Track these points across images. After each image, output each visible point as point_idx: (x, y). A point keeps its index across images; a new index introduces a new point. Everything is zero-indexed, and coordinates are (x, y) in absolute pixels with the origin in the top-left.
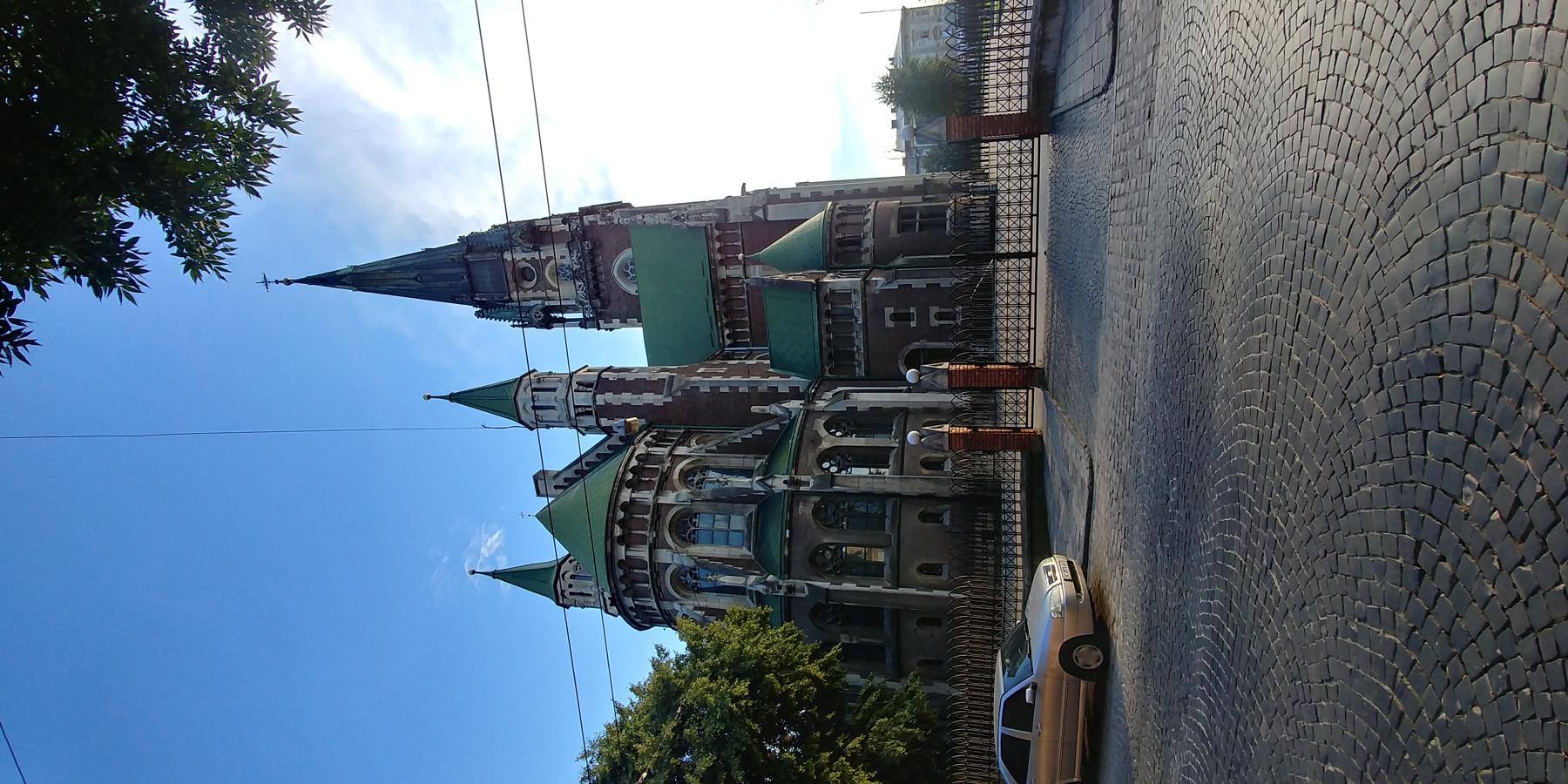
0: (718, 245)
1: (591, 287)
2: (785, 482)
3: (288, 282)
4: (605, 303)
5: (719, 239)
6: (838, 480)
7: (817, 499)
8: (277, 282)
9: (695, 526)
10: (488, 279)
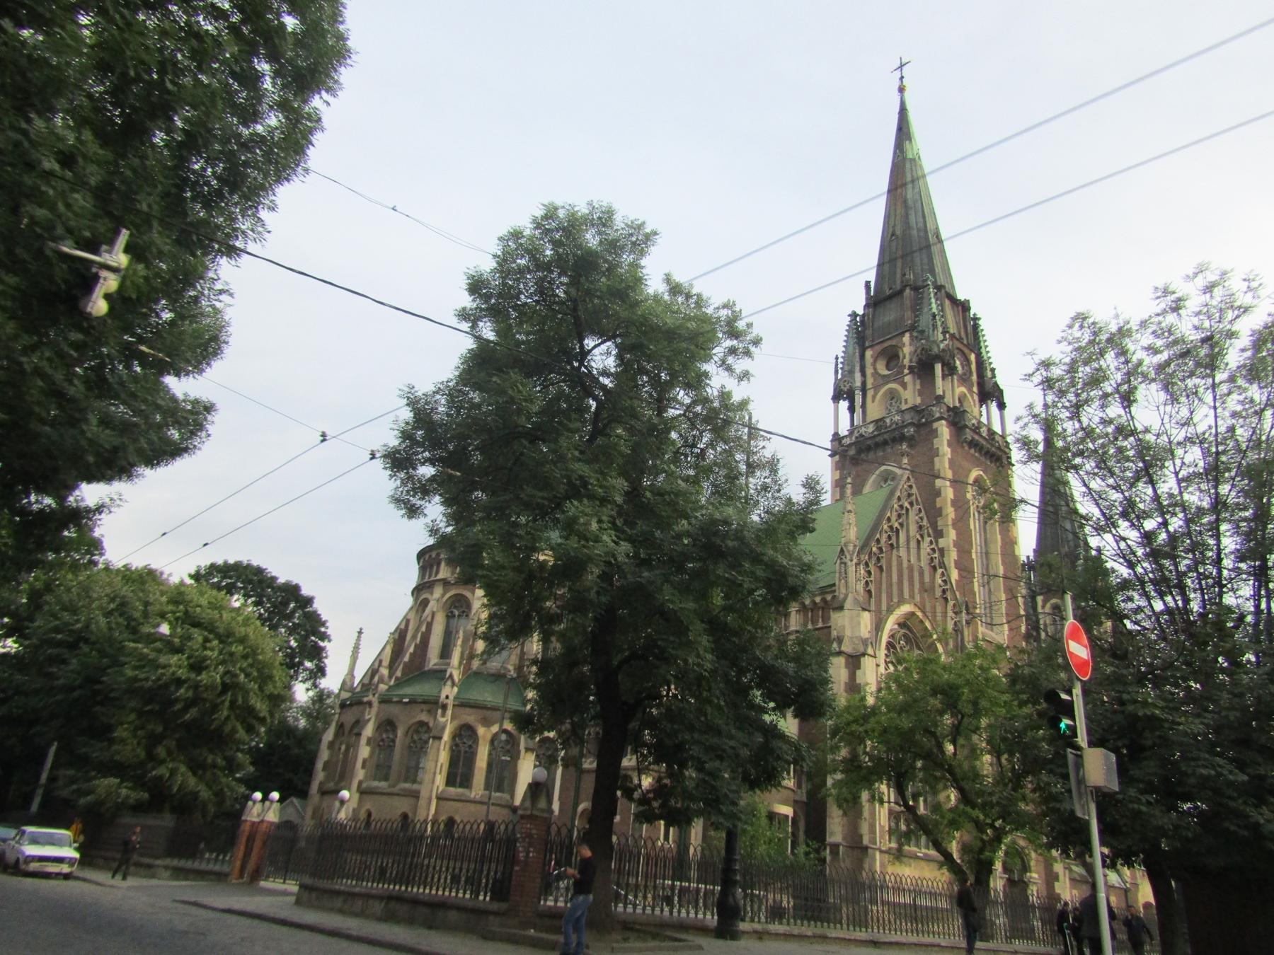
0: (818, 599)
1: (869, 442)
2: (447, 697)
3: (901, 90)
4: (855, 461)
5: (824, 600)
6: (437, 742)
7: (431, 725)
8: (902, 78)
9: (459, 616)
10: (886, 319)
